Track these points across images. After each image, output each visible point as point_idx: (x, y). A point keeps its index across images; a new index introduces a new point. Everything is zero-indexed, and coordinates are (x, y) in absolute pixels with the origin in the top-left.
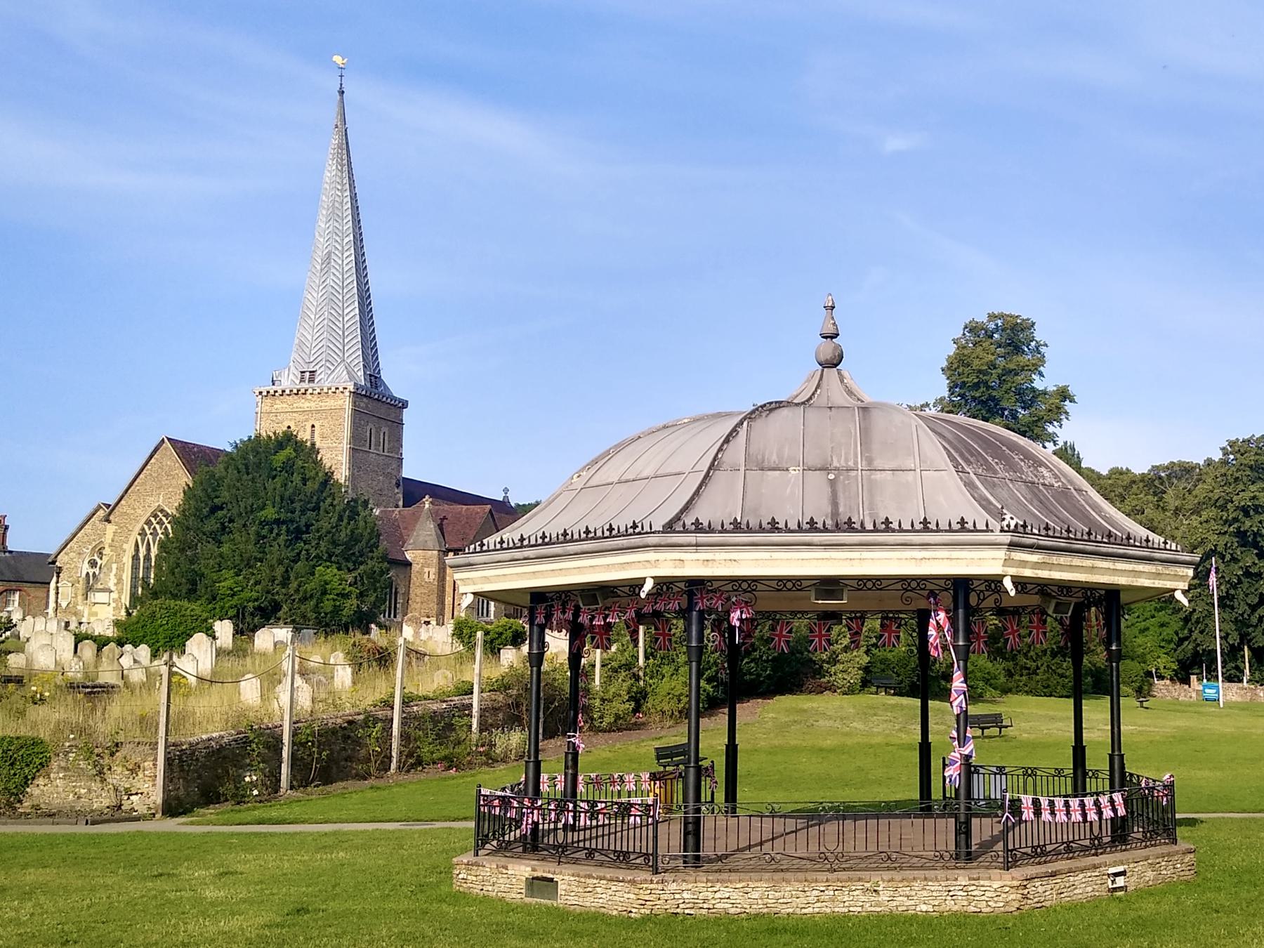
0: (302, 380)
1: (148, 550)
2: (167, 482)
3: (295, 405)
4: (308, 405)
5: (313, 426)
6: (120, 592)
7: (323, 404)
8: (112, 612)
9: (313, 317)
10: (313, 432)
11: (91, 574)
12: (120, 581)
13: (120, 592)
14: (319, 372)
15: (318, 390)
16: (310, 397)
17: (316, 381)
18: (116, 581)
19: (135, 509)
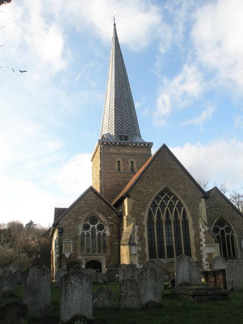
4: (128, 151)
5: (132, 162)
10: (132, 165)
13: (143, 246)
15: (134, 144)
19: (147, 189)
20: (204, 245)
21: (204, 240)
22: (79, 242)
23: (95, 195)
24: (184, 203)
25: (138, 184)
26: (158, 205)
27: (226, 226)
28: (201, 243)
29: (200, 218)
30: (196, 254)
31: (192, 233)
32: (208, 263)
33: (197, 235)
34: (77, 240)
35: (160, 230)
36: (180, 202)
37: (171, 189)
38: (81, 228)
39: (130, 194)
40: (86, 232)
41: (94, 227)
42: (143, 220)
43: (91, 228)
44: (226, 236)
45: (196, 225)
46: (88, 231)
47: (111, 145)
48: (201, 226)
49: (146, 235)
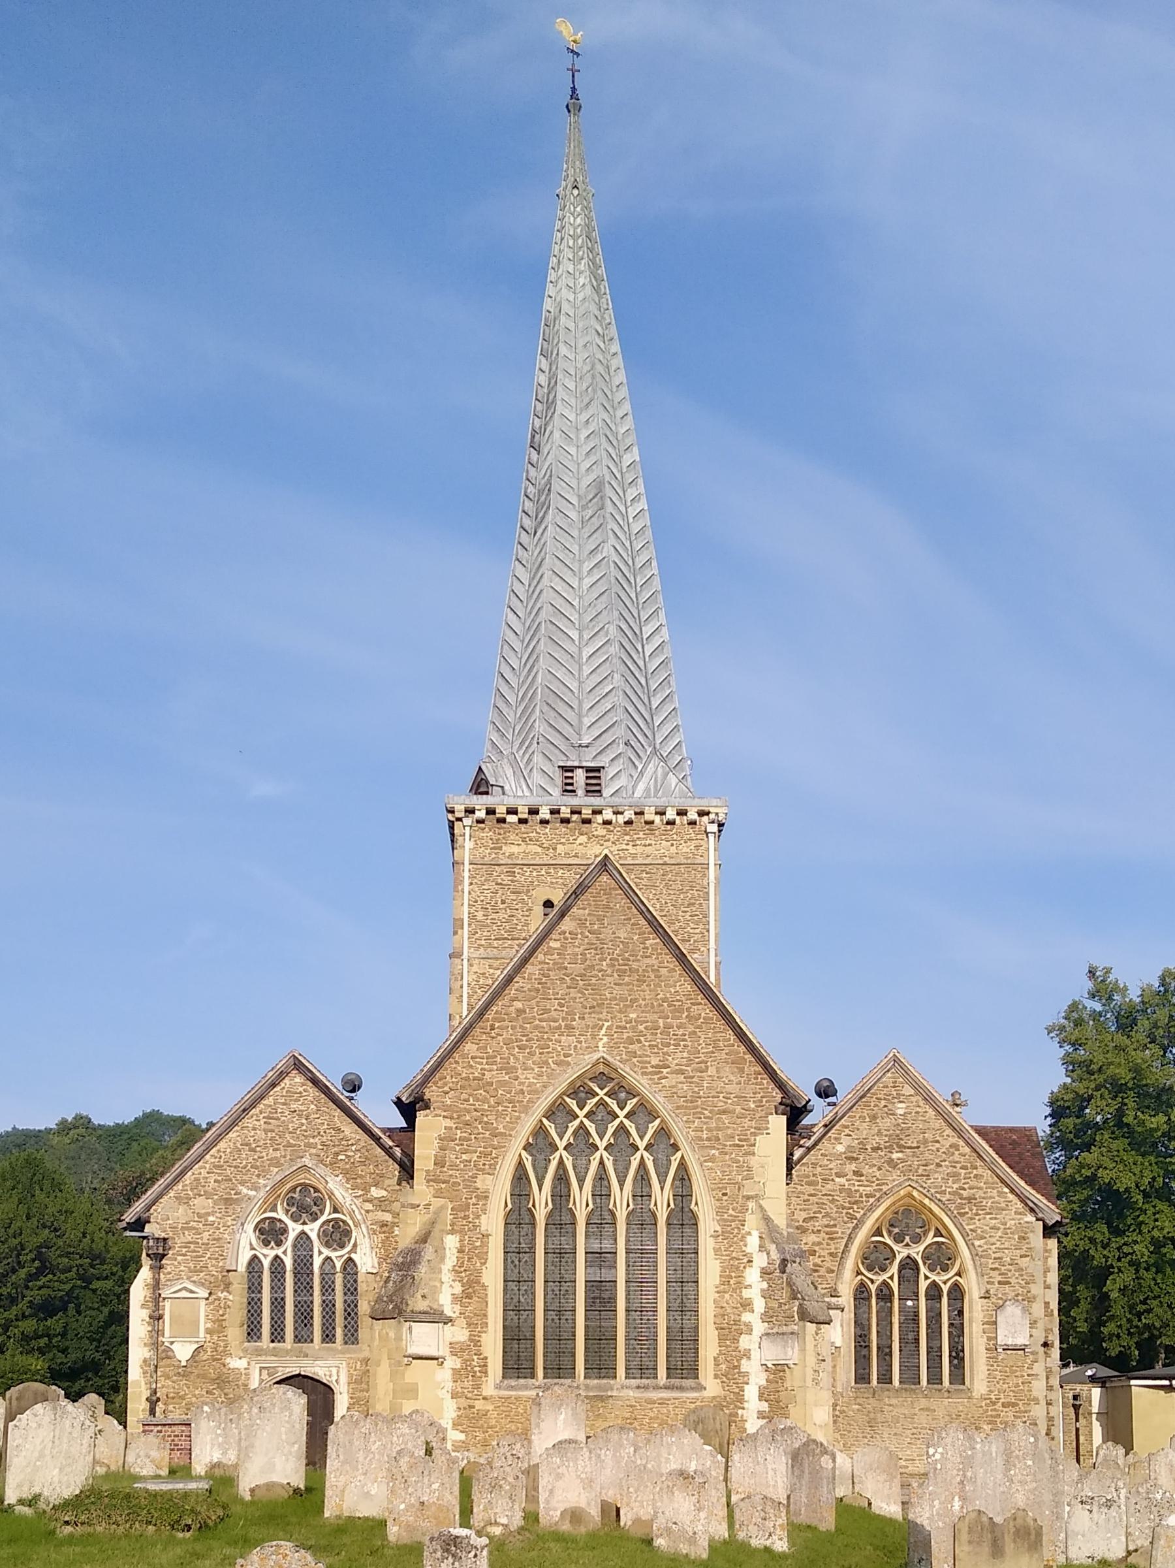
0: (568, 789)
1: (602, 1192)
2: (617, 991)
3: (560, 848)
6: (477, 1323)
7: (640, 849)
8: (449, 1385)
9: (574, 635)
11: (266, 1263)
12: (471, 1288)
13: (477, 1323)
14: (611, 771)
15: (629, 815)
16: (601, 831)
17: (606, 792)
18: (458, 1289)
19: (509, 1070)
20: (759, 1328)
21: (759, 1305)
22: (237, 1297)
23: (313, 1092)
24: (680, 1133)
25: (469, 1047)
26: (561, 1144)
27: (930, 1239)
28: (746, 1317)
29: (751, 1205)
30: (717, 1365)
31: (710, 1270)
32: (764, 1406)
33: (732, 1278)
34: (227, 1286)
35: (561, 1256)
36: (663, 1132)
37: (625, 1069)
38: (248, 1236)
39: (430, 1093)
40: (267, 1255)
41: (303, 1236)
42: (484, 1211)
43: (292, 1236)
44: (923, 1285)
45: (730, 1233)
46: (279, 1252)
47: (512, 819)
48: (753, 1242)
49: (493, 1275)
